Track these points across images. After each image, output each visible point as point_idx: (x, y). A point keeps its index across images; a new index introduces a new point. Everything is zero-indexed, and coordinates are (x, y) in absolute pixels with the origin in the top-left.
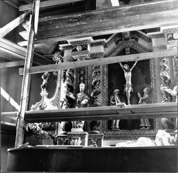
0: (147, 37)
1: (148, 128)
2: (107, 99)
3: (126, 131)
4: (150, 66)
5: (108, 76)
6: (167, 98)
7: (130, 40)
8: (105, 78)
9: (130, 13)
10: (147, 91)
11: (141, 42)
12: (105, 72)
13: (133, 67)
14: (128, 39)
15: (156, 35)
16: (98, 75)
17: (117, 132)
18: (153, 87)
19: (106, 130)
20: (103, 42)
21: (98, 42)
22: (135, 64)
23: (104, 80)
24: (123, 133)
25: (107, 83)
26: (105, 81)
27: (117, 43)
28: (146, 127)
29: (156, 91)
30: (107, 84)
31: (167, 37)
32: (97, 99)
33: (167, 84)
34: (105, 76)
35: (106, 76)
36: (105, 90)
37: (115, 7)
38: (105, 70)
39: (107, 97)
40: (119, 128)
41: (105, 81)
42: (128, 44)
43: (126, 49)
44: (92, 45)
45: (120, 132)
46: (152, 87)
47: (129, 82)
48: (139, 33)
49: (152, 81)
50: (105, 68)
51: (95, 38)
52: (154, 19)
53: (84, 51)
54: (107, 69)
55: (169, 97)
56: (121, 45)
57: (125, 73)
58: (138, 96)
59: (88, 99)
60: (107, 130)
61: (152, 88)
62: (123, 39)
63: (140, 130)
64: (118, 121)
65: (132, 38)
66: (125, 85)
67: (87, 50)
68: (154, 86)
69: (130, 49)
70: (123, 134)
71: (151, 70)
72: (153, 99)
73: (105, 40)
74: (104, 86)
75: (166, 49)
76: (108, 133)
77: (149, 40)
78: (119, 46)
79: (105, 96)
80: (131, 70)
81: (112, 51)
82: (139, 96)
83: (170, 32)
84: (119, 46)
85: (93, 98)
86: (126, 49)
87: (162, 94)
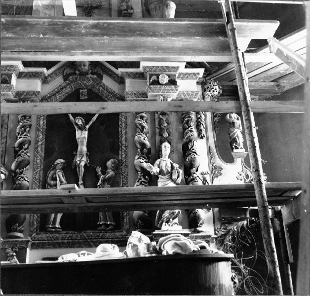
0: (117, 75)
1: (110, 227)
2: (42, 175)
3: (73, 232)
4: (120, 123)
5: (46, 135)
6: (144, 178)
7: (90, 76)
8: (41, 137)
9: (94, 31)
11: (107, 81)
12: (42, 127)
13: (91, 123)
14: (87, 74)
15: (132, 73)
16: (27, 131)
17: (57, 235)
18: (123, 159)
19: (36, 232)
20: (41, 73)
21: (32, 73)
22: (95, 118)
23: (38, 142)
24: (67, 236)
25: (43, 146)
26: (40, 143)
27: (66, 78)
28: (107, 226)
29: (126, 167)
30: (44, 149)
31: (150, 80)
32: (22, 175)
33: (145, 156)
34: (40, 134)
35: (43, 135)
36: (38, 159)
37: (70, 17)
38: (41, 123)
39: (42, 172)
40: (60, 227)
41: (40, 143)
42: (85, 82)
43: (81, 91)
44: (20, 75)
45: (63, 235)
46: (120, 158)
47: (83, 148)
48: (105, 66)
49: (121, 149)
51: (26, 64)
52: (132, 48)
53: (5, 85)
54: (45, 121)
55: (147, 177)
56: (74, 83)
58: (97, 173)
59: (5, 175)
60: (38, 231)
62: (77, 72)
63: (97, 231)
64: (59, 216)
65: (92, 73)
66: (77, 152)
67: (10, 83)
68: (124, 156)
69: (88, 91)
70: (66, 239)
71: (120, 129)
72: (122, 178)
73: (44, 70)
74: (37, 152)
75: (147, 97)
76: (40, 236)
77: (121, 80)
78: (69, 84)
79: (39, 170)
80: (87, 127)
81: (56, 90)
82: (100, 173)
83: (155, 71)
84: (69, 84)
85: (14, 172)
86: (81, 91)
87: (137, 171)
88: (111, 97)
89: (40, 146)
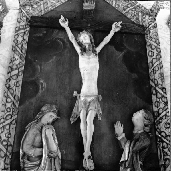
2: (13, 132)
4: (149, 49)
5: (26, 59)
8: (17, 62)
10: (147, 122)
12: (20, 46)
18: (160, 111)
23: (12, 70)
25: (20, 78)
26: (15, 72)
30: (21, 83)
34: (17, 57)
35: (20, 58)
36: (9, 100)
39: (13, 126)
41: (15, 72)
46: (155, 109)
47: (89, 87)
49: (154, 92)
50: (22, 35)
54: (26, 37)
57: (80, 57)
61: (156, 114)
66: (79, 92)
71: (149, 59)
79: (8, 122)
80: (99, 49)
88: (132, 9)
89: (14, 77)
